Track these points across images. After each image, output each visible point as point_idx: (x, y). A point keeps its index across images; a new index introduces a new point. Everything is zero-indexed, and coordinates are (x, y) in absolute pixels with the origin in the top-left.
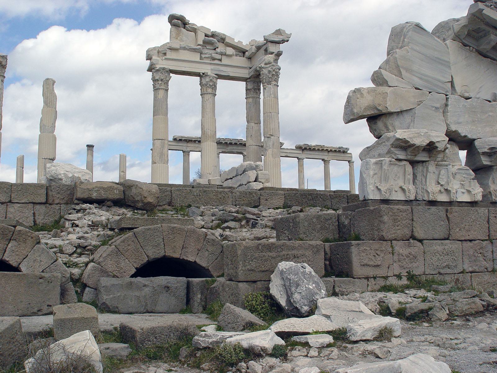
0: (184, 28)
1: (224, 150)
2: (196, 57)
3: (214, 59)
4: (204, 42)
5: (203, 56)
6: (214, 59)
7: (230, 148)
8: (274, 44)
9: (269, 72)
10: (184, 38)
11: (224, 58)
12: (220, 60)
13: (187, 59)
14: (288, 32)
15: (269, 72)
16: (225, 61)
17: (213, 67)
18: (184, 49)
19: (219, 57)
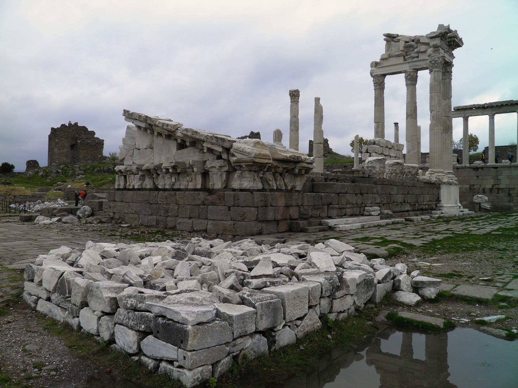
0: (393, 41)
1: (497, 112)
2: (401, 60)
3: (414, 58)
4: (405, 47)
5: (406, 57)
6: (414, 58)
7: (503, 109)
8: (434, 39)
9: (430, 62)
10: (393, 48)
11: (420, 55)
12: (418, 57)
13: (394, 63)
14: (446, 25)
15: (430, 62)
16: (422, 57)
17: (411, 64)
18: (392, 57)
19: (416, 55)
